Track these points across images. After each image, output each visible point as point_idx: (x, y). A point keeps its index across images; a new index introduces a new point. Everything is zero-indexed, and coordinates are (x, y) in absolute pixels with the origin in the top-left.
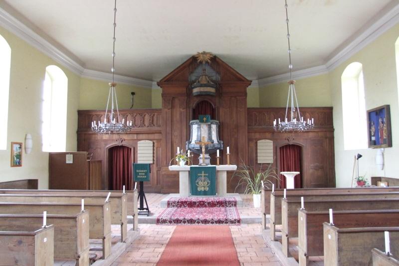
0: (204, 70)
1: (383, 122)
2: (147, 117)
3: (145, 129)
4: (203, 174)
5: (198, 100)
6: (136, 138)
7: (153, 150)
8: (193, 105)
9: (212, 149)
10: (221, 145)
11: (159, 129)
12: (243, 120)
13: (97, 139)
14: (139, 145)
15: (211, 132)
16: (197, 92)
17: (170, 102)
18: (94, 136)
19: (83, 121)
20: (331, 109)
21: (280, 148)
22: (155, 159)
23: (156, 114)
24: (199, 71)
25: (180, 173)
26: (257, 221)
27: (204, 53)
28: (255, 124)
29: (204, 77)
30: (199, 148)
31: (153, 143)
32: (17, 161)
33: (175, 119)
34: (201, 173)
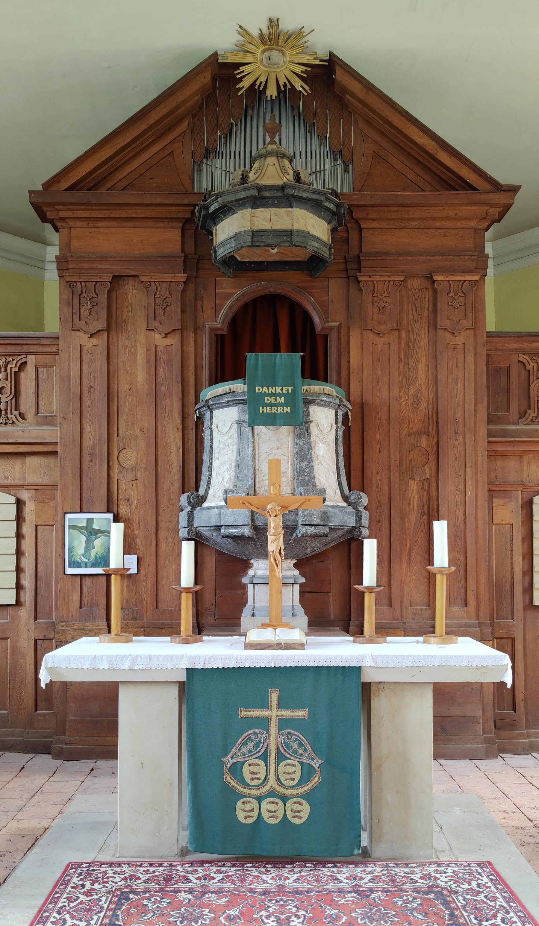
4: (274, 713)
5: (239, 292)
7: (19, 536)
8: (217, 316)
9: (314, 537)
10: (359, 516)
11: (47, 433)
15: (309, 445)
16: (236, 236)
17: (103, 298)
22: (27, 582)
23: (31, 360)
25: (125, 699)
28: (522, 415)
30: (246, 531)
31: (20, 504)
34: (265, 705)
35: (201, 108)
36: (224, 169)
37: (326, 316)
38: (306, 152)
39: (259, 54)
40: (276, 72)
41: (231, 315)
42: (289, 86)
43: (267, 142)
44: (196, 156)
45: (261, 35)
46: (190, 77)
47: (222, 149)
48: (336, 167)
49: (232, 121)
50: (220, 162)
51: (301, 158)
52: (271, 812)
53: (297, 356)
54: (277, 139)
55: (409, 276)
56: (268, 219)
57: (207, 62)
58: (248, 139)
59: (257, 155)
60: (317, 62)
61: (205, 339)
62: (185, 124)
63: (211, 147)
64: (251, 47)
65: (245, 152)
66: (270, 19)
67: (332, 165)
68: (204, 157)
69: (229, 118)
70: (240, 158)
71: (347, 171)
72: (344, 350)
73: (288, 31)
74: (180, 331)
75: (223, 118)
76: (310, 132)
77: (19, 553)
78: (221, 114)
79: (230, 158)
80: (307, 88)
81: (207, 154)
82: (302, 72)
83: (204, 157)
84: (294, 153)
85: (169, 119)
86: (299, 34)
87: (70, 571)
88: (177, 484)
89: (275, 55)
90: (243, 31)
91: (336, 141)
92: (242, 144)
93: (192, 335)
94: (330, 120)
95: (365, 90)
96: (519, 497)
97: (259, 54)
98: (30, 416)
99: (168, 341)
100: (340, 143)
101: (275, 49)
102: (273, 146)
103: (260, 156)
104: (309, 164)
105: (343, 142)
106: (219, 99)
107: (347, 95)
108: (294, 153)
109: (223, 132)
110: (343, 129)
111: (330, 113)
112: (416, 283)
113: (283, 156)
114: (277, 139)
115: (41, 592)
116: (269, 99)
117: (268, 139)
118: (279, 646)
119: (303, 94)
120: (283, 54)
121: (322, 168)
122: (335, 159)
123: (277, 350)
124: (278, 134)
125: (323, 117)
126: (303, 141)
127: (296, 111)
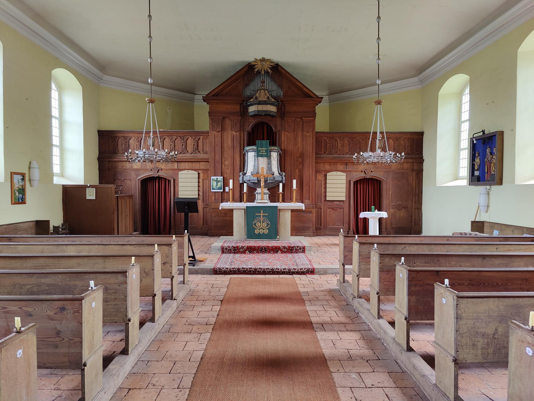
0: (263, 82)
1: (491, 153)
2: (190, 142)
3: (187, 156)
6: (176, 168)
7: (199, 182)
8: (249, 128)
10: (282, 178)
11: (205, 156)
12: (309, 147)
13: (125, 168)
14: (180, 176)
18: (120, 164)
19: (108, 147)
20: (421, 134)
21: (356, 183)
23: (201, 137)
24: (256, 84)
25: (234, 211)
26: (331, 272)
27: (263, 60)
29: (262, 91)
30: (256, 181)
31: (199, 174)
32: (19, 198)
33: (225, 145)
37: (276, 128)
52: (262, 232)
53: (268, 141)
55: (296, 118)
56: (261, 108)
72: (280, 137)
77: (199, 186)
87: (212, 191)
88: (239, 170)
96: (323, 173)
98: (201, 152)
112: (298, 120)
115: (204, 196)
118: (263, 203)
123: (264, 139)
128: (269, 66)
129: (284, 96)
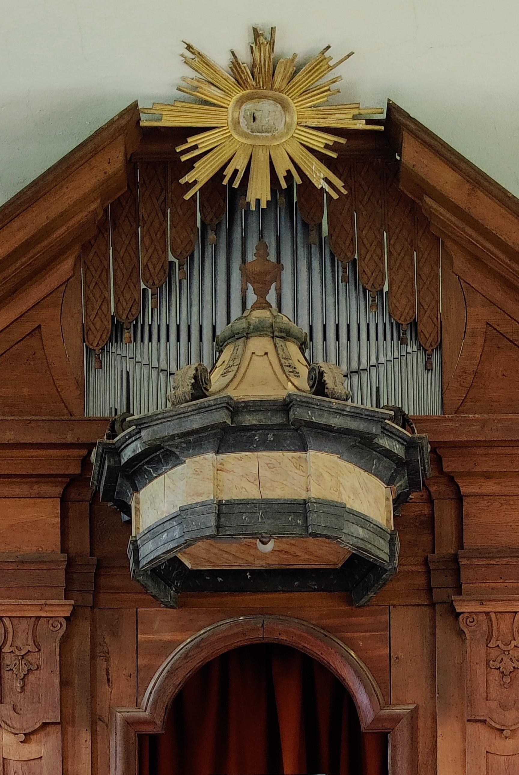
5: (188, 641)
16: (182, 515)
27: (262, 71)
35: (101, 228)
36: (155, 364)
37: (385, 690)
38: (337, 326)
39: (230, 107)
40: (268, 147)
41: (171, 692)
42: (297, 179)
43: (250, 303)
44: (91, 337)
45: (236, 65)
46: (78, 161)
47: (148, 321)
48: (403, 359)
49: (171, 258)
50: (146, 350)
51: (325, 339)
54: (271, 298)
57: (114, 126)
58: (209, 297)
59: (227, 334)
60: (361, 125)
61: (116, 746)
62: (67, 265)
63: (124, 317)
64: (213, 94)
65: (201, 327)
66: (255, 30)
67: (396, 355)
68: (110, 339)
69: (165, 251)
70: (189, 340)
71: (428, 367)
73: (295, 55)
74: (59, 727)
75: (150, 250)
76: (345, 280)
78: (147, 242)
79: (168, 340)
80: (338, 183)
81: (116, 331)
82: (327, 146)
83: (110, 339)
84: (311, 328)
85: (31, 254)
86: (320, 62)
89: (267, 109)
90: (194, 56)
91: (404, 301)
92: (195, 309)
93: (85, 736)
94: (390, 253)
95: (467, 186)
97: (230, 107)
99: (32, 750)
100: (413, 305)
101: (266, 97)
102: (264, 314)
103: (234, 336)
104: (344, 354)
105: (420, 304)
106: (142, 211)
107: (427, 199)
108: (311, 328)
109: (151, 282)
110: (419, 275)
111: (389, 239)
113: (287, 334)
114: (271, 298)
116: (253, 208)
117: (252, 298)
119: (329, 197)
120: (285, 107)
121: (373, 361)
122: (402, 341)
124: (273, 286)
125: (373, 247)
126: (330, 300)
127: (314, 235)
128: (320, 141)
129: (459, 397)
